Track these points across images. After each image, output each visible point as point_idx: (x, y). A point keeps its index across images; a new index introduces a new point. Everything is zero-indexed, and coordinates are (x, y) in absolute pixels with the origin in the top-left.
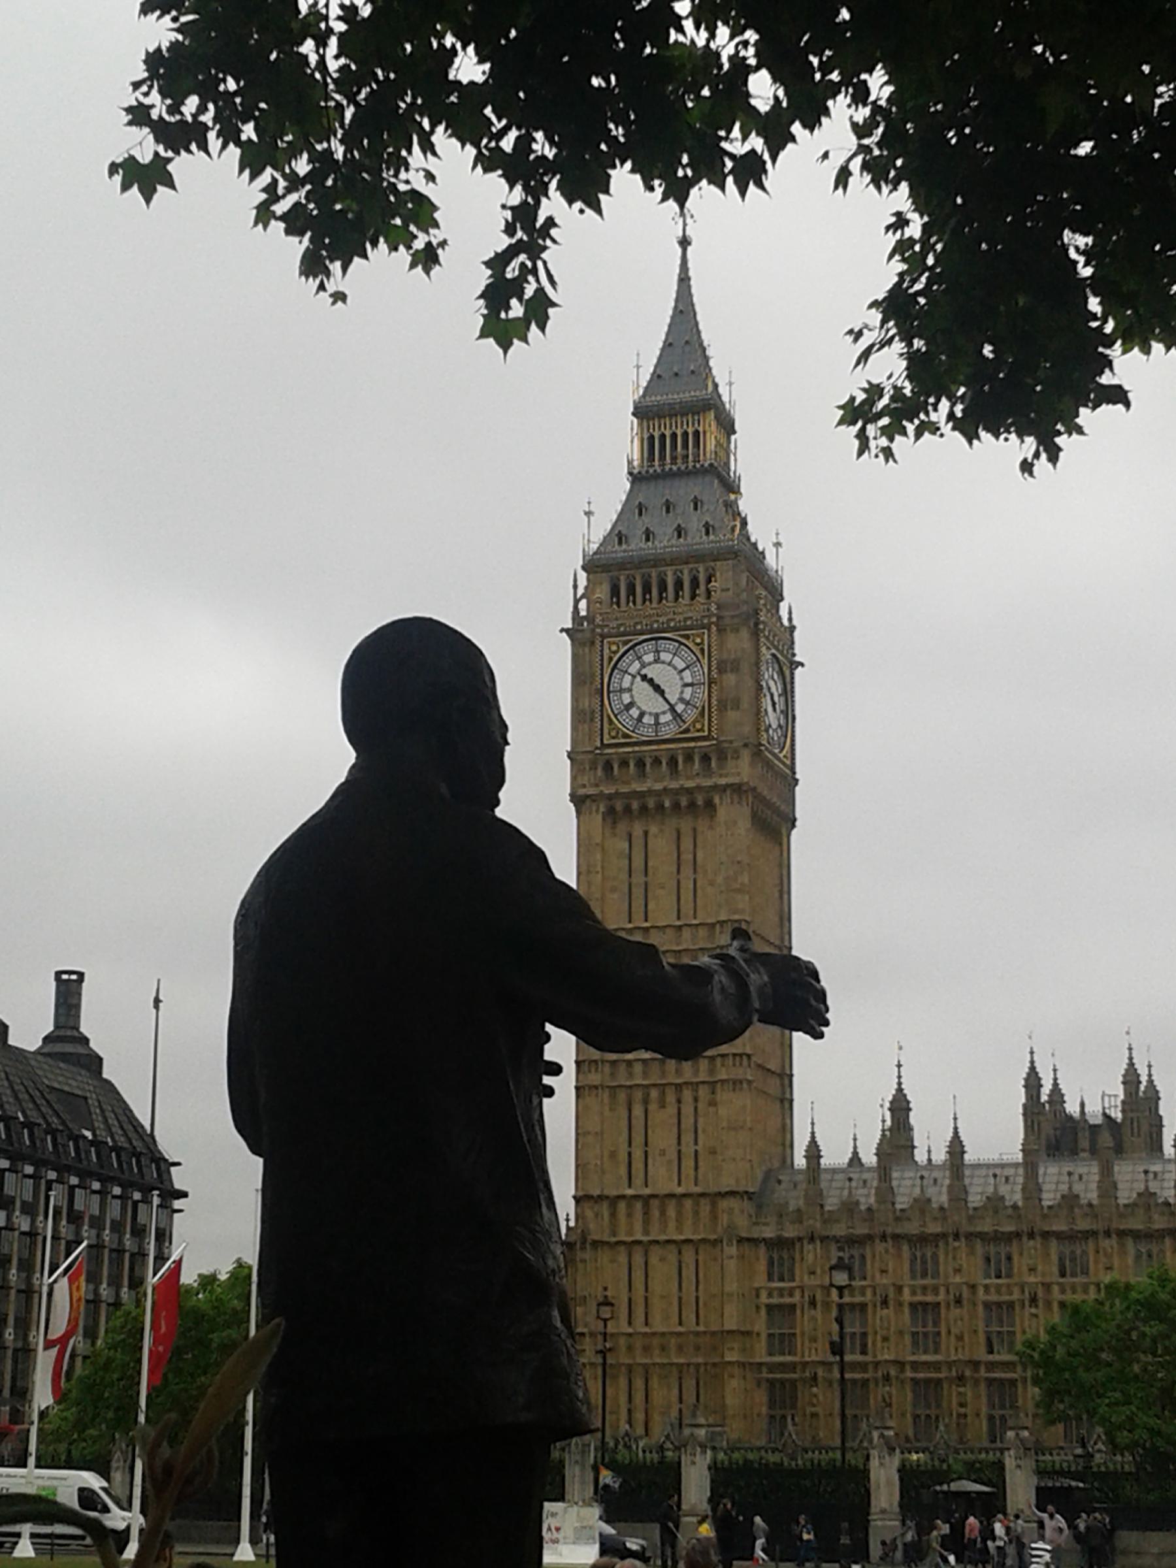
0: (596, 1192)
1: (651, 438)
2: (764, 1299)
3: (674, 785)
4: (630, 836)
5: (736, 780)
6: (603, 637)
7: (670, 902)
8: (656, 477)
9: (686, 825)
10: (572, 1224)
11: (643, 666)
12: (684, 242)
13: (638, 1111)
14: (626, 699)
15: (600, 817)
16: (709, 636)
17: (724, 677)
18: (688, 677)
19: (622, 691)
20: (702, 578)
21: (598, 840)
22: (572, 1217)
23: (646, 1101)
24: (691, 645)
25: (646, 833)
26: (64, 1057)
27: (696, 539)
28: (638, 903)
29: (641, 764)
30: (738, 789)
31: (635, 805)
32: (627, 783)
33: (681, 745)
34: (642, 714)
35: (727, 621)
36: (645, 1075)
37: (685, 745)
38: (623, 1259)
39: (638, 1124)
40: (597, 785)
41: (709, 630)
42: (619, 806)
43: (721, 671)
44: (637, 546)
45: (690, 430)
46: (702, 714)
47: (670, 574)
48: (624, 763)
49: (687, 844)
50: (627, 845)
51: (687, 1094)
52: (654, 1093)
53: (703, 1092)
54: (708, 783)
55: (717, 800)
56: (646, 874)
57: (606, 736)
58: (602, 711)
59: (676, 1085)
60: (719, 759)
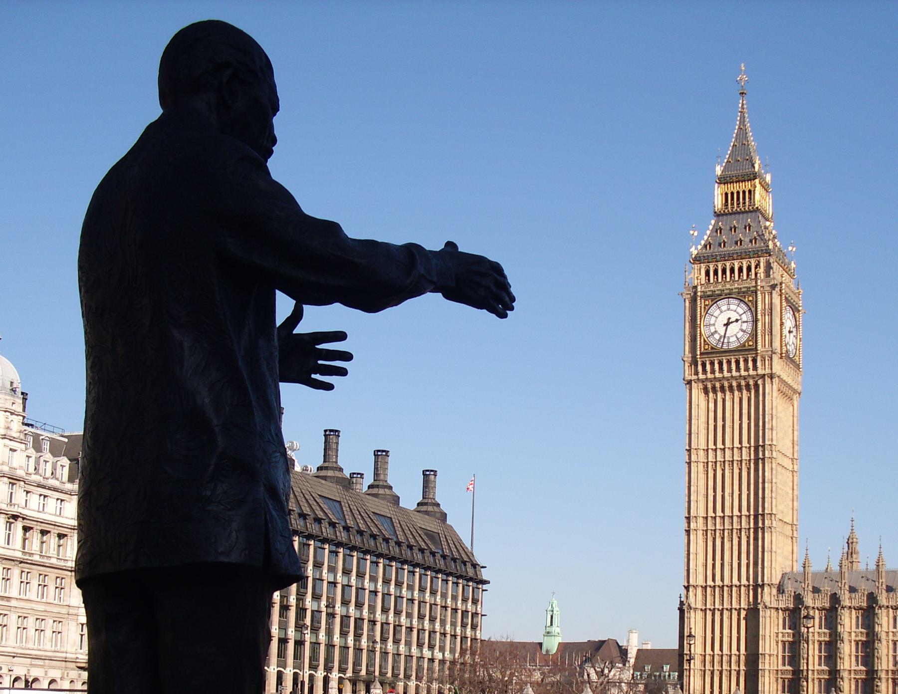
1: (726, 194)
2: (780, 638)
14: (712, 329)
18: (744, 318)
26: (427, 513)
30: (771, 376)
44: (716, 250)
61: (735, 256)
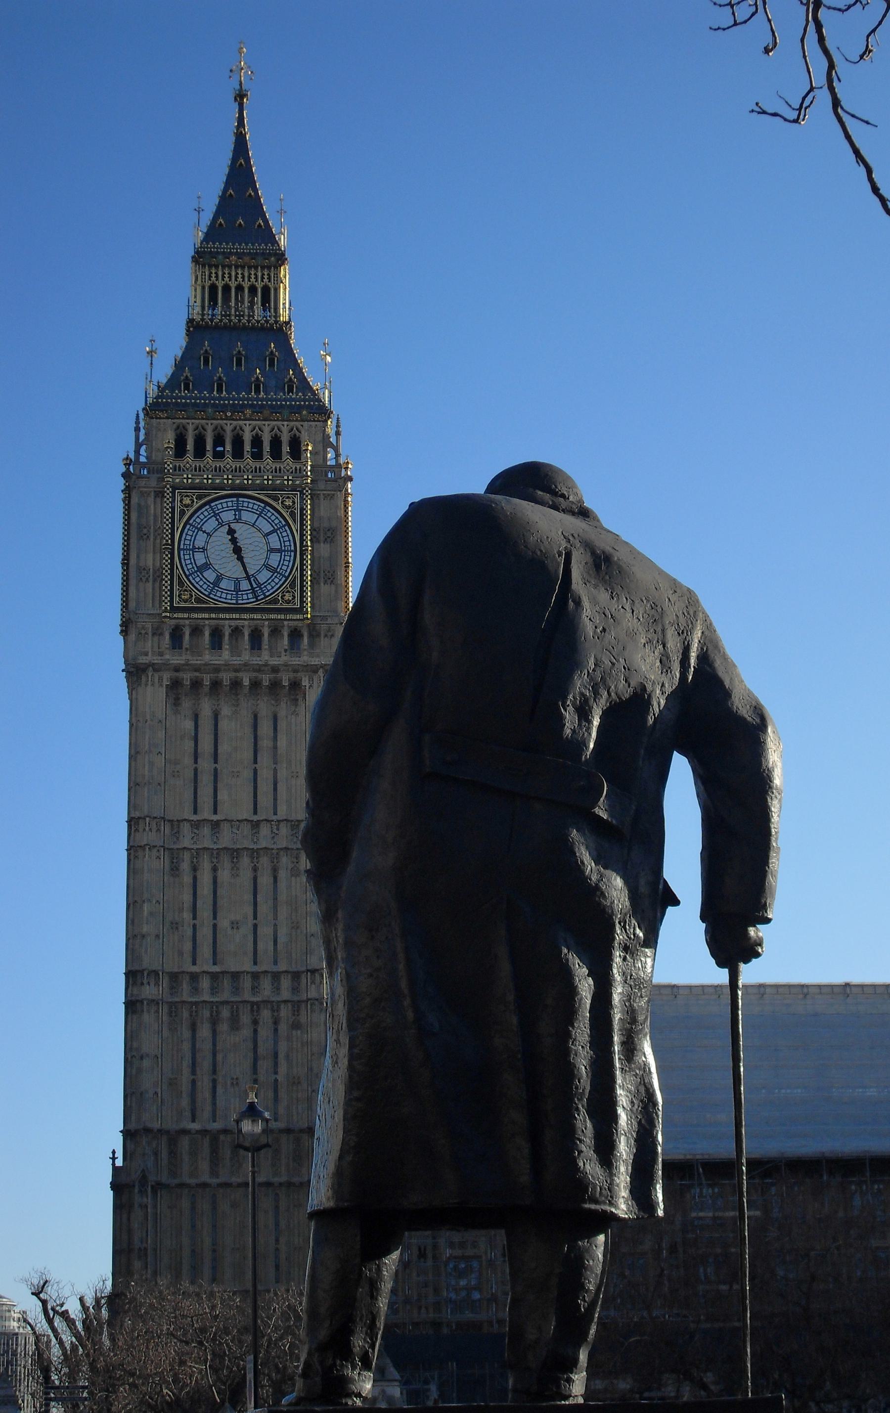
0: (156, 1125)
1: (213, 288)
3: (256, 661)
6: (174, 488)
9: (264, 707)
10: (119, 1163)
11: (238, 520)
12: (240, 96)
13: (204, 1032)
14: (200, 559)
16: (302, 499)
20: (285, 438)
22: (120, 1154)
23: (214, 1022)
24: (279, 507)
28: (205, 792)
29: (217, 634)
34: (219, 578)
35: (321, 485)
36: (214, 990)
37: (272, 616)
38: (185, 1204)
39: (205, 1046)
41: (302, 493)
42: (187, 677)
45: (259, 285)
46: (293, 585)
48: (196, 631)
49: (265, 728)
50: (189, 725)
51: (266, 1014)
52: (225, 1013)
53: (285, 1012)
54: (296, 661)
55: (305, 682)
56: (216, 762)
57: (176, 599)
58: (172, 569)
59: (253, 1004)
60: (311, 636)
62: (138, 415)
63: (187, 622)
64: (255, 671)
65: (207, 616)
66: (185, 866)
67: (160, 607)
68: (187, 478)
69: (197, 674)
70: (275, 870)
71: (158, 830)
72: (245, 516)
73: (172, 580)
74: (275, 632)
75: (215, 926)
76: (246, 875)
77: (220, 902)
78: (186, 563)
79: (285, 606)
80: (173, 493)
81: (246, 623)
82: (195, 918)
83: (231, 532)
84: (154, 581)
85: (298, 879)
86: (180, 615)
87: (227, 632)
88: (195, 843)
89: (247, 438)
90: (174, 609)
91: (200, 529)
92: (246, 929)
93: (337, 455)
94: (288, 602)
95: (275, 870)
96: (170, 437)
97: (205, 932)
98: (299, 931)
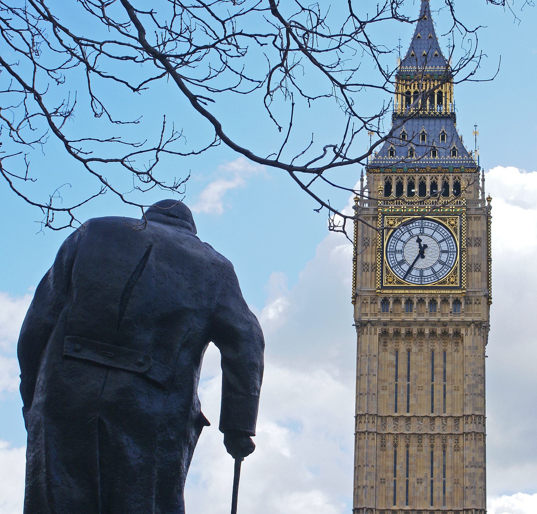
4: (397, 352)
5: (476, 319)
7: (425, 400)
8: (412, 117)
9: (438, 347)
11: (422, 234)
15: (376, 338)
16: (461, 220)
17: (469, 248)
19: (396, 252)
20: (451, 183)
21: (375, 352)
24: (447, 225)
25: (409, 351)
27: (444, 158)
29: (409, 302)
31: (403, 331)
32: (399, 314)
33: (439, 292)
35: (472, 211)
37: (443, 292)
40: (376, 315)
41: (461, 216)
42: (391, 330)
43: (468, 244)
47: (428, 178)
48: (397, 301)
49: (439, 360)
50: (393, 358)
54: (458, 319)
55: (463, 332)
56: (409, 380)
57: (385, 281)
58: (382, 264)
60: (466, 303)
61: (428, 169)
62: (362, 171)
63: (391, 295)
64: (432, 325)
65: (403, 292)
66: (389, 444)
67: (375, 286)
68: (391, 208)
69: (397, 327)
70: (444, 447)
71: (373, 422)
72: (426, 231)
73: (382, 270)
74: (445, 301)
75: (407, 481)
76: (426, 450)
77: (410, 467)
78: (391, 260)
79: (451, 285)
80: (383, 217)
81: (427, 296)
82: (395, 476)
83: (419, 241)
84: (372, 270)
85: (458, 452)
86: (387, 291)
87: (415, 301)
88: (396, 430)
89: (428, 183)
90: (383, 288)
91: (399, 239)
92: (426, 483)
93: (483, 193)
94: (452, 283)
95: (444, 447)
96: (381, 184)
97: (401, 484)
98: (458, 485)
